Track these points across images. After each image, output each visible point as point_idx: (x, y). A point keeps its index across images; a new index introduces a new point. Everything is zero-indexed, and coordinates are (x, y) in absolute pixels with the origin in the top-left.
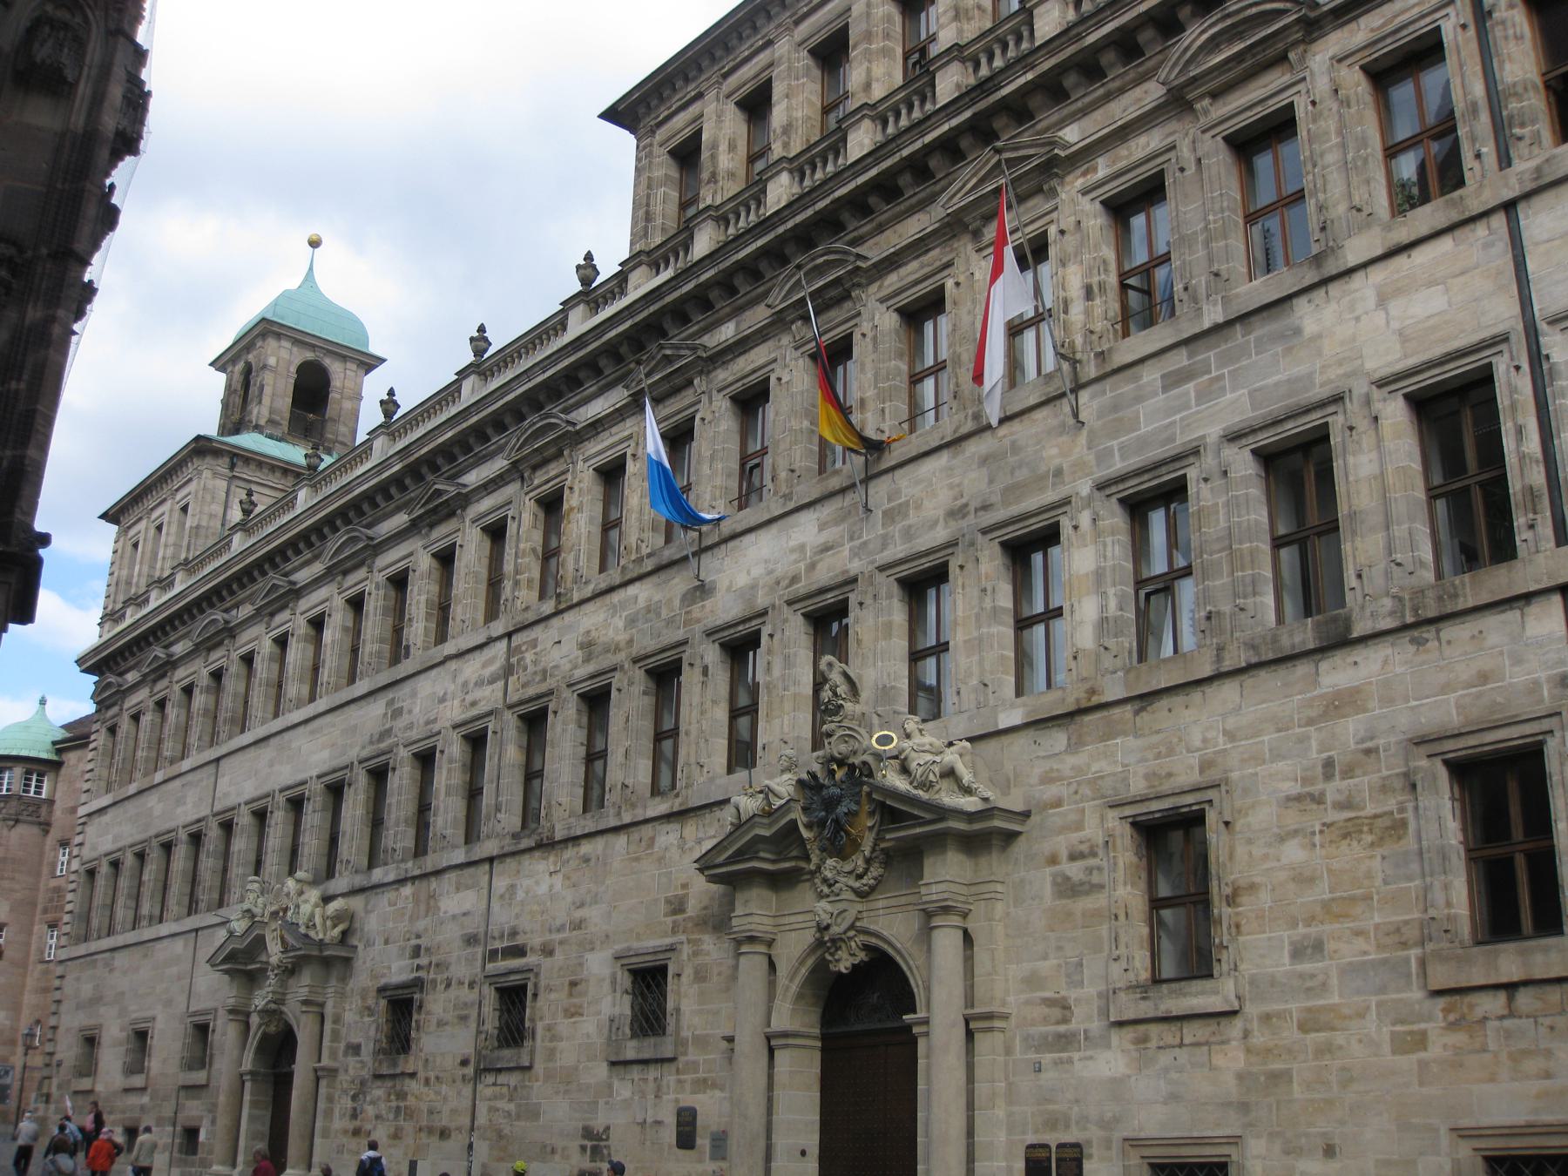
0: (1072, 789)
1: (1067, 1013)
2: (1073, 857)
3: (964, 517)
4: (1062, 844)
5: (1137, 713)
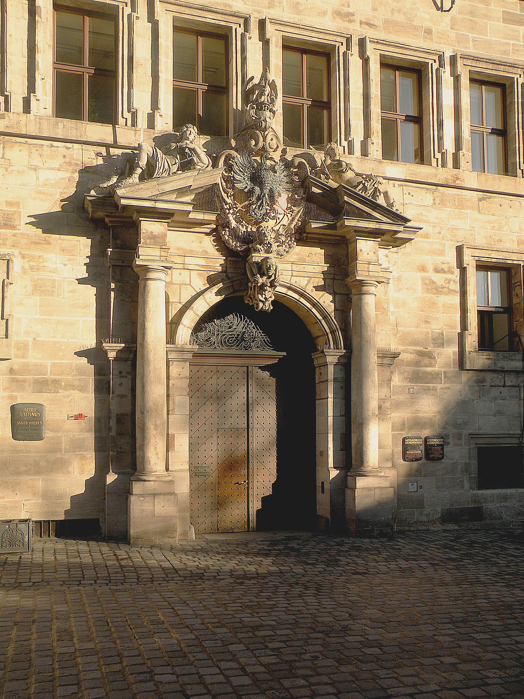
0: (438, 229)
1: (433, 361)
2: (437, 270)
3: (350, 21)
4: (430, 261)
5: (480, 200)
